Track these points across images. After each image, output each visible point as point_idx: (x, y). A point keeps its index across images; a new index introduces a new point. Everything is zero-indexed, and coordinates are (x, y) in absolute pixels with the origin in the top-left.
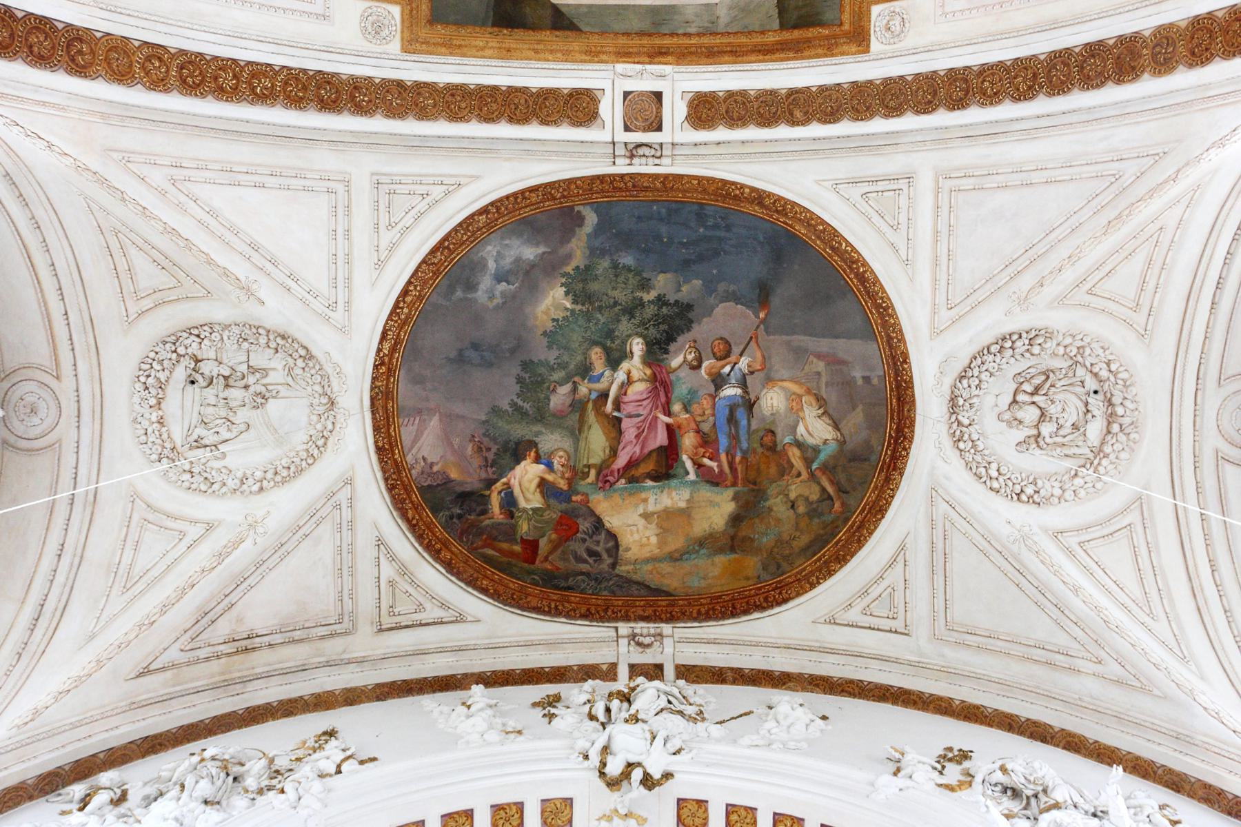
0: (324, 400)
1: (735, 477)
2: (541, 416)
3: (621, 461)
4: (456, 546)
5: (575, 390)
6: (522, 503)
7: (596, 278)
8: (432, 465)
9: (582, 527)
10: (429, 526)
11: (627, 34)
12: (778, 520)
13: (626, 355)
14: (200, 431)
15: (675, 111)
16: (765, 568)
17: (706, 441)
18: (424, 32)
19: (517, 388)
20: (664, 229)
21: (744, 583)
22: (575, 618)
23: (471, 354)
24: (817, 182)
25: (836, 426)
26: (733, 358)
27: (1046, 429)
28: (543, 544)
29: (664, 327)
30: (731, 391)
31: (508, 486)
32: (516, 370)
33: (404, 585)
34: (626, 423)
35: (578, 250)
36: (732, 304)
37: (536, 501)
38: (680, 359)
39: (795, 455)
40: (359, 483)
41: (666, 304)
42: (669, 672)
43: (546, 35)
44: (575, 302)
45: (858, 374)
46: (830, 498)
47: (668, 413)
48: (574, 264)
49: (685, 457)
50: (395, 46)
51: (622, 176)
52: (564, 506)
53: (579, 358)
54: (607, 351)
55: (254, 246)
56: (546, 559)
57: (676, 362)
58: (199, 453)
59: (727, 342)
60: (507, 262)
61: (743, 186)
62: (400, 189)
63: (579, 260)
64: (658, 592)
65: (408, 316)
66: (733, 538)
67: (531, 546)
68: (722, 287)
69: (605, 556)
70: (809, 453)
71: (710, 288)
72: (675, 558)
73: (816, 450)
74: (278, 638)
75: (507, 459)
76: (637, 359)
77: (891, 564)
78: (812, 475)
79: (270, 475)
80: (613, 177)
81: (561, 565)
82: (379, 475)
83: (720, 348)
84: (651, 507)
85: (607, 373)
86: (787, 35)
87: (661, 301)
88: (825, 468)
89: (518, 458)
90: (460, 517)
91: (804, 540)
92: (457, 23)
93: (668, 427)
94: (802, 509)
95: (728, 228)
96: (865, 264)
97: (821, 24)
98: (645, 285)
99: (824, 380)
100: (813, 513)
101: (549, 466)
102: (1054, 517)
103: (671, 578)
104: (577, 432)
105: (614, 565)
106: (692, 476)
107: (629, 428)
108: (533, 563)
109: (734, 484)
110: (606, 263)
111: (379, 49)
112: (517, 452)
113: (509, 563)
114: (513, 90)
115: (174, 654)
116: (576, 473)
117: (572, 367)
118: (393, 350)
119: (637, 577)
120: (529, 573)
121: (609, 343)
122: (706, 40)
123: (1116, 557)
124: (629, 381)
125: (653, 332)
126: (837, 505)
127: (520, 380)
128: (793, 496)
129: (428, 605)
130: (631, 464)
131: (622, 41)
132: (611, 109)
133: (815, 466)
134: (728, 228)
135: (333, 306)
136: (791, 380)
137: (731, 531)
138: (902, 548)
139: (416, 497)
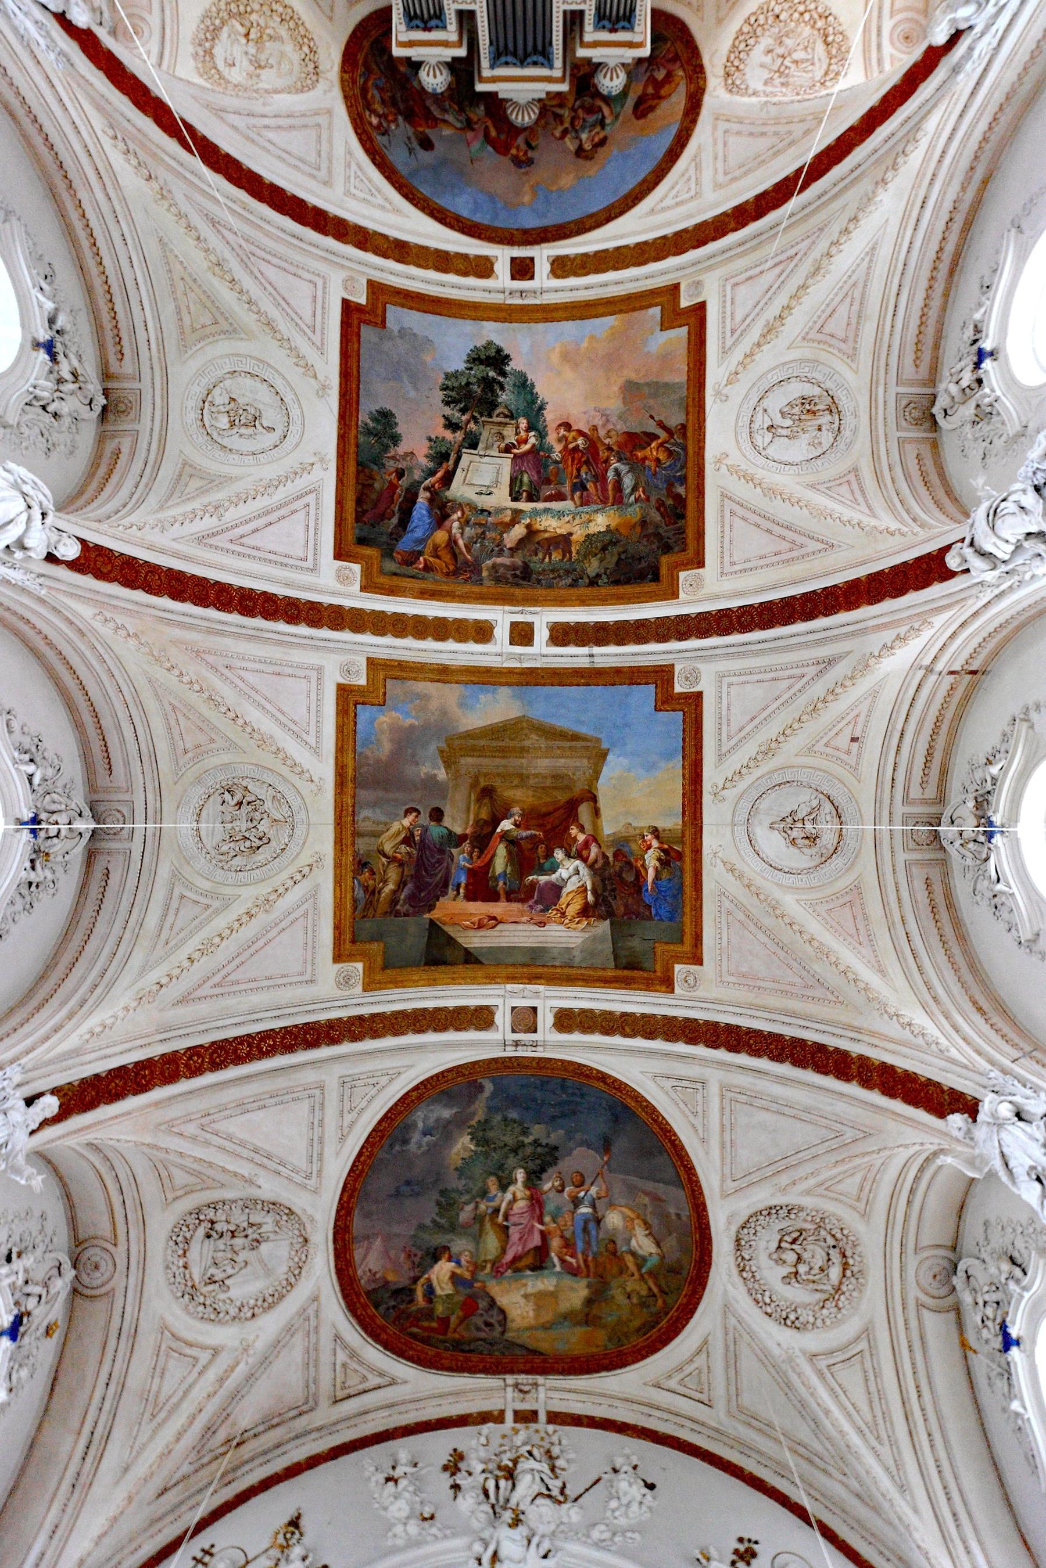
0: (301, 1240)
1: (588, 1271)
2: (453, 1228)
3: (509, 1257)
4: (392, 1329)
5: (476, 1208)
7: (492, 1128)
8: (375, 1274)
9: (481, 1306)
10: (372, 1318)
11: (513, 965)
12: (619, 1306)
13: (513, 1181)
14: (212, 1270)
15: (546, 1019)
16: (610, 1340)
17: (568, 1244)
18: (378, 977)
19: (436, 1209)
20: (538, 1095)
21: (595, 1350)
22: (475, 1372)
23: (405, 1189)
25: (658, 1244)
26: (585, 1187)
27: (802, 1269)
28: (454, 1320)
29: (538, 1162)
30: (585, 1210)
31: (429, 1280)
32: (435, 1196)
33: (354, 1365)
34: (512, 1230)
35: (479, 1110)
36: (584, 1149)
37: (449, 1289)
39: (629, 1260)
40: (323, 1299)
41: (540, 1145)
42: (542, 1417)
43: (460, 968)
44: (477, 1145)
45: (672, 1211)
46: (654, 1295)
47: (542, 1223)
48: (477, 1119)
49: (553, 1254)
50: (359, 989)
52: (468, 1291)
53: (480, 1184)
54: (500, 1179)
56: (455, 1331)
57: (547, 1186)
58: (211, 1287)
59: (582, 1176)
60: (431, 1122)
61: (592, 1069)
62: (358, 1083)
63: (480, 1115)
64: (535, 1352)
65: (362, 1171)
66: (587, 1315)
67: (445, 1321)
68: (578, 1136)
69: (497, 1326)
70: (640, 1260)
71: (570, 1135)
72: (546, 1327)
73: (644, 1259)
74: (261, 1428)
75: (428, 1260)
76: (520, 1184)
77: (699, 1352)
78: (642, 1276)
79: (260, 1303)
80: (503, 1060)
81: (466, 1334)
82: (338, 1288)
83: (577, 1179)
84: (530, 1290)
86: (619, 973)
87: (536, 1143)
88: (650, 1273)
89: (436, 1259)
90: (394, 1307)
91: (637, 1323)
92: (400, 967)
93: (542, 1232)
95: (582, 1096)
96: (675, 1134)
97: (641, 969)
98: (525, 1132)
99: (650, 1209)
100: (643, 1304)
101: (458, 1263)
102: (811, 1341)
103: (545, 1343)
104: (478, 1237)
105: (503, 1333)
106: (558, 1269)
107: (514, 1233)
108: (445, 1334)
109: (588, 1276)
111: (348, 993)
112: (435, 1255)
113: (429, 1337)
114: (437, 1010)
115: (186, 1469)
116: (477, 1267)
117: (474, 1192)
118: (351, 1196)
119: (519, 1341)
120: (444, 1342)
121: (500, 1173)
122: (566, 971)
124: (515, 1199)
125: (531, 1165)
126: (660, 1302)
127: (438, 1204)
128: (629, 1289)
129: (370, 1376)
130: (516, 1259)
131: (511, 970)
132: (503, 1019)
133: (644, 1270)
134: (582, 1096)
135: (308, 1177)
136: (626, 1206)
137: (586, 1310)
138: (706, 1342)
139: (364, 1299)
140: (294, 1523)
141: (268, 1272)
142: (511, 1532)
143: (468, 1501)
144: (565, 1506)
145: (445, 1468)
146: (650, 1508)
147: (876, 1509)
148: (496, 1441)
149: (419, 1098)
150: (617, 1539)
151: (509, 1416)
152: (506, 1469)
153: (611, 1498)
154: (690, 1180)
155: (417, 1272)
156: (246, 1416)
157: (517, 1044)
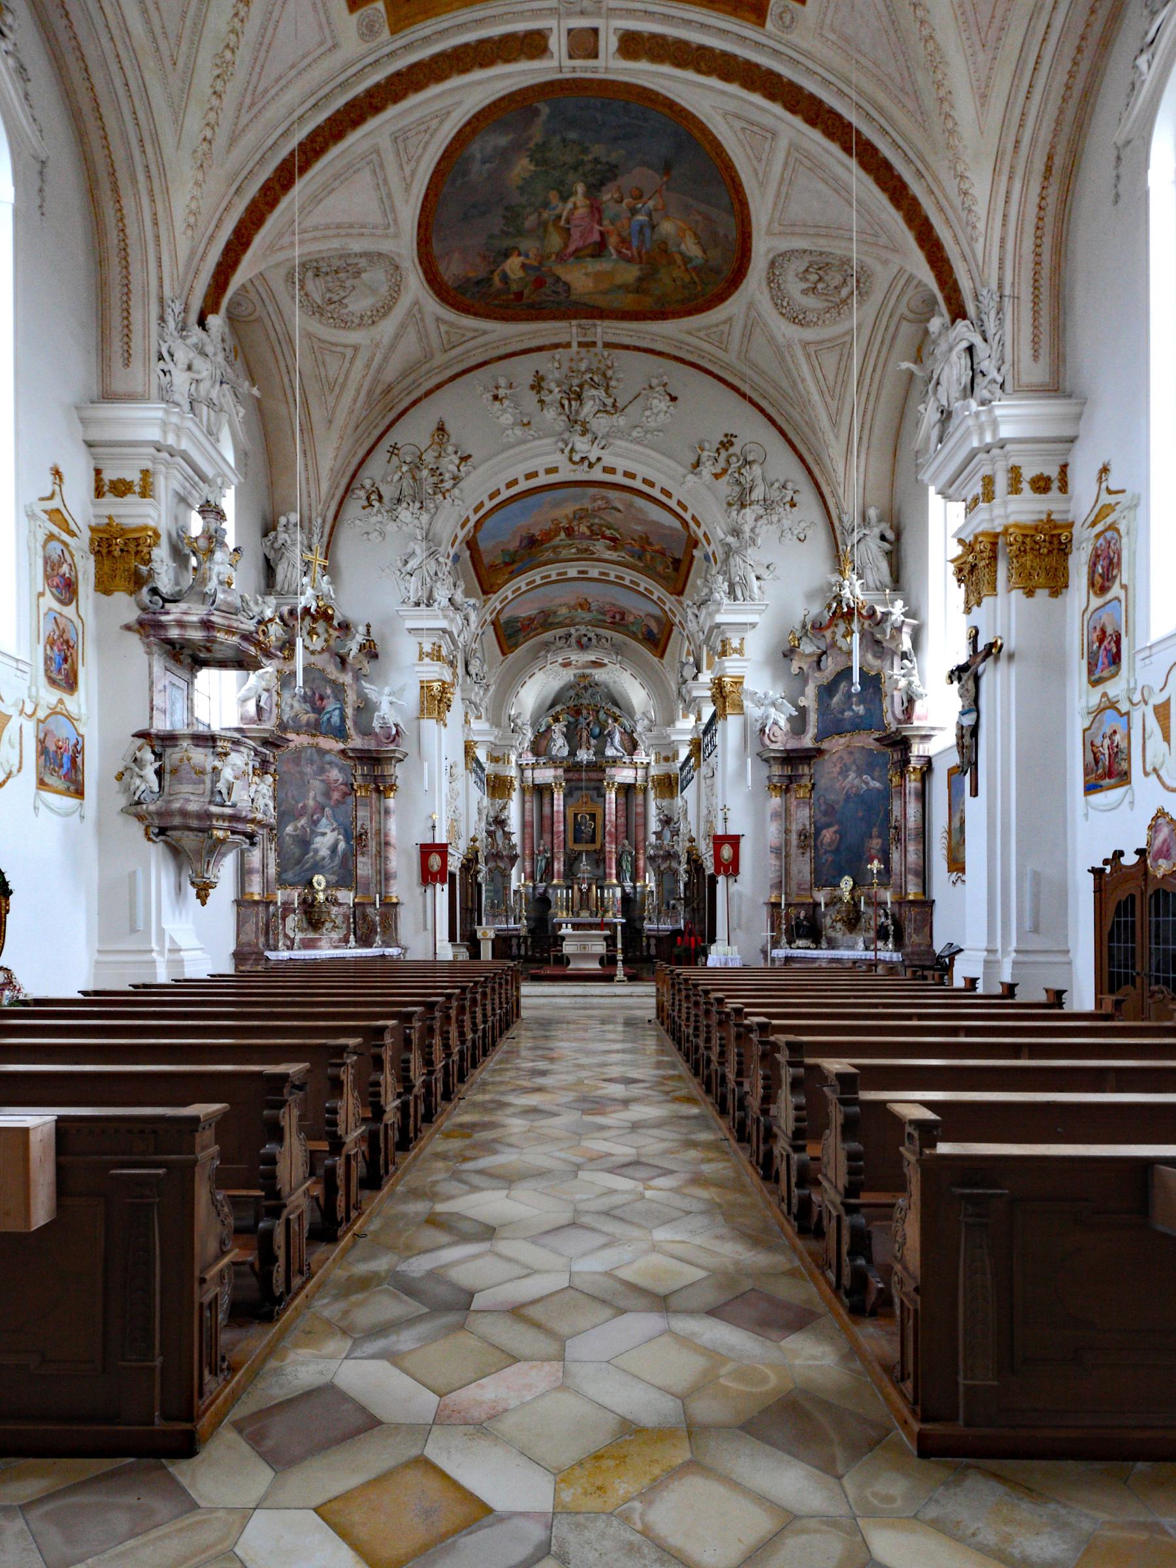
2: (520, 233)
3: (572, 248)
6: (512, 276)
13: (573, 193)
14: (328, 295)
17: (624, 241)
24: (713, 107)
25: (704, 252)
26: (644, 199)
27: (820, 286)
28: (526, 292)
30: (641, 218)
35: (537, 133)
37: (521, 274)
38: (608, 196)
42: (600, 344)
44: (537, 165)
45: (721, 232)
47: (601, 225)
50: (386, 34)
51: (568, 80)
54: (560, 192)
57: (606, 197)
58: (333, 306)
62: (409, 134)
70: (687, 260)
73: (690, 260)
80: (560, 81)
82: (431, 292)
84: (590, 269)
85: (560, 205)
87: (596, 161)
88: (695, 268)
94: (679, 283)
98: (585, 151)
100: (684, 287)
101: (527, 256)
102: (809, 334)
103: (601, 302)
106: (615, 256)
107: (576, 233)
110: (557, 138)
111: (374, 44)
112: (506, 254)
114: (481, 42)
118: (426, 230)
123: (830, 361)
124: (575, 207)
125: (591, 180)
126: (699, 288)
127: (504, 217)
130: (576, 251)
133: (689, 266)
140: (441, 429)
141: (374, 291)
142: (581, 438)
143: (550, 414)
145: (532, 387)
147: (814, 432)
148: (566, 365)
149: (474, 132)
151: (575, 345)
152: (575, 392)
154: (742, 213)
155: (492, 267)
156: (389, 376)
157: (574, 69)
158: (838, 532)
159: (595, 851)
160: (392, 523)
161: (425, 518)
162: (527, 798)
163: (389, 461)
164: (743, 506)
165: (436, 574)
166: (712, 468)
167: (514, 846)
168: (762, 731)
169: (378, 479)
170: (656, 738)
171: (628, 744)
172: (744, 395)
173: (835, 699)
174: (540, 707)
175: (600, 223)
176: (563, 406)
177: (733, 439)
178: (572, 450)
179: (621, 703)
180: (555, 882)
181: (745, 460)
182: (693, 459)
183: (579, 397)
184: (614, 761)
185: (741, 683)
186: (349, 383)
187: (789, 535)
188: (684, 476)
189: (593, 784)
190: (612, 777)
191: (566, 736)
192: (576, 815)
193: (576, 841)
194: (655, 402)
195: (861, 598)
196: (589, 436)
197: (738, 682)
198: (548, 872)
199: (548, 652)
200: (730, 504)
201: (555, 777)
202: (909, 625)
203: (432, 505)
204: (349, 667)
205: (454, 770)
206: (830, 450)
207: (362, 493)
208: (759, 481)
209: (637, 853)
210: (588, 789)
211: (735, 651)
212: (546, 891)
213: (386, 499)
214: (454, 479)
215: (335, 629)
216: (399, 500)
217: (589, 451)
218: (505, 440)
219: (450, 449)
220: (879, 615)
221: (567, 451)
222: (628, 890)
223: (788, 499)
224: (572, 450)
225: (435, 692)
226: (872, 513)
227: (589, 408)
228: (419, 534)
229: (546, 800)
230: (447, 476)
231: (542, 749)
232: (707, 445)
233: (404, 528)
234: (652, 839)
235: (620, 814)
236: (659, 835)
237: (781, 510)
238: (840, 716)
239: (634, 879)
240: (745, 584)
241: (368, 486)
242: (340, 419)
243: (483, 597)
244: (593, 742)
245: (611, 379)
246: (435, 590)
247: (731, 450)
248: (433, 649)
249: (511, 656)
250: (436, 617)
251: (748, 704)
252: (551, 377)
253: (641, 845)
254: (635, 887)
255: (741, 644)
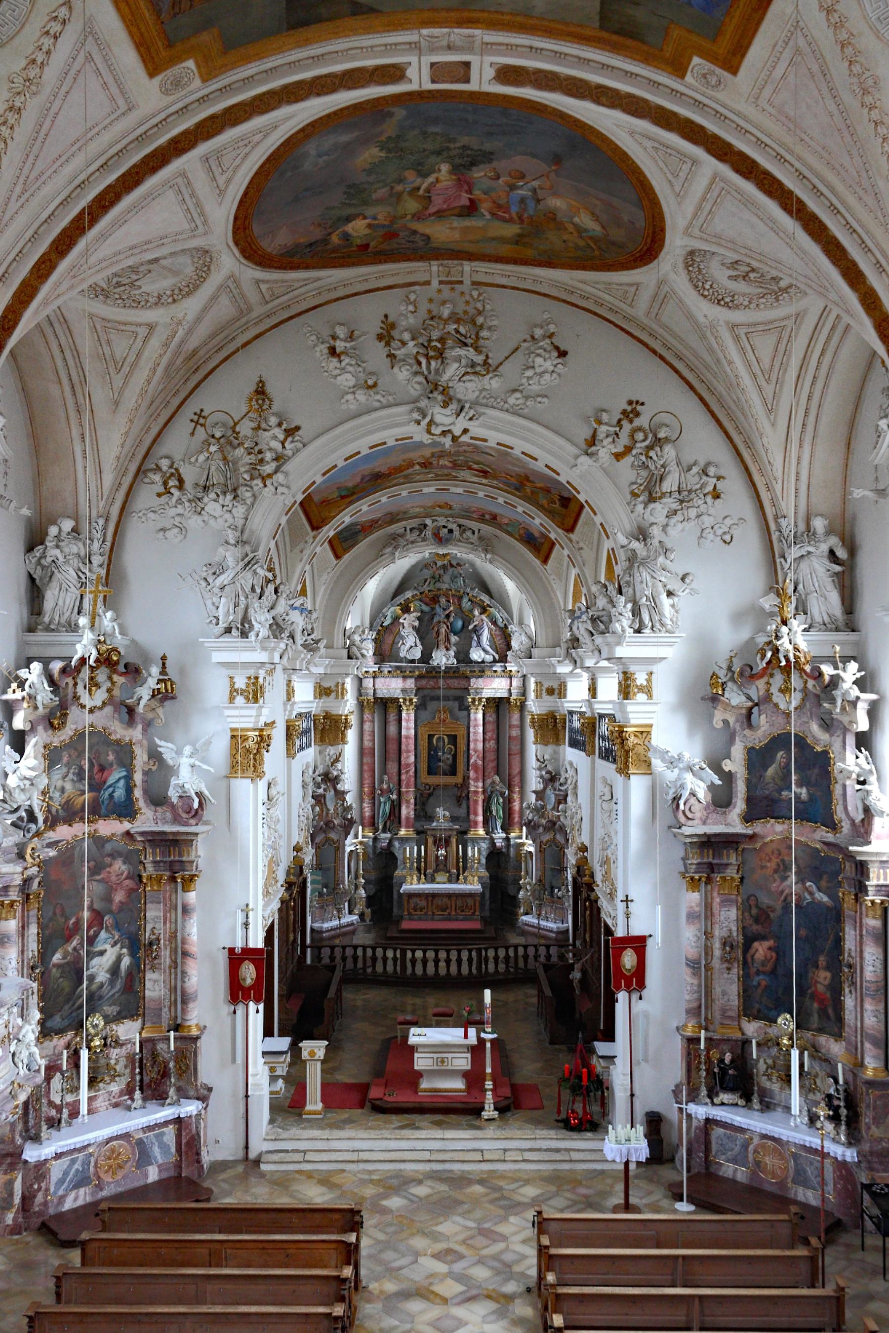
26: (526, 180)
55: (132, 248)
79: (176, 292)
102: (737, 316)
123: (765, 345)
140: (261, 391)
143: (402, 374)
144: (488, 377)
146: (559, 375)
147: (745, 417)
148: (424, 307)
150: (528, 403)
152: (435, 348)
153: (528, 368)
155: (330, 230)
156: (193, 342)
158: (775, 537)
159: (456, 785)
160: (196, 517)
161: (240, 511)
162: (367, 716)
163: (192, 434)
164: (652, 499)
165: (253, 589)
166: (612, 446)
167: (350, 808)
168: (676, 799)
169: (177, 457)
170: (538, 665)
171: (499, 641)
172: (654, 352)
173: (771, 771)
174: (384, 590)
175: (470, 191)
176: (419, 363)
177: (639, 408)
178: (431, 423)
179: (492, 586)
180: (403, 832)
181: (655, 436)
182: (588, 434)
183: (440, 355)
184: (482, 669)
185: (649, 733)
186: (142, 363)
187: (711, 536)
188: (577, 457)
189: (451, 693)
190: (478, 691)
191: (417, 630)
192: (430, 737)
193: (430, 772)
194: (539, 361)
195: (803, 646)
196: (454, 406)
197: (645, 733)
198: (394, 818)
199: (396, 548)
200: (634, 495)
201: (404, 691)
202: (865, 701)
203: (248, 494)
204: (138, 719)
205: (273, 792)
206: (765, 440)
207: (157, 478)
208: (673, 467)
209: (511, 791)
210: (446, 698)
211: (641, 689)
212: (390, 843)
213: (188, 485)
214: (276, 459)
215: (121, 674)
216: (205, 488)
217: (453, 424)
218: (344, 407)
219: (273, 420)
220: (827, 678)
221: (424, 423)
222: (499, 843)
223: (710, 488)
224: (431, 423)
225: (250, 744)
226: (819, 524)
227: (452, 370)
228: (231, 537)
229: (392, 717)
230: (268, 456)
231: (386, 647)
232: (605, 417)
233: (212, 522)
234: (532, 798)
235: (489, 735)
236: (540, 795)
237: (700, 502)
238: (775, 795)
239: (506, 828)
240: (655, 606)
241: (165, 468)
242: (130, 399)
243: (312, 534)
244: (454, 639)
245: (481, 327)
246: (251, 611)
247: (637, 422)
248: (248, 685)
249: (347, 557)
250: (253, 649)
251: (658, 765)
252: (404, 323)
253: (517, 780)
254: (507, 839)
255: (649, 681)
